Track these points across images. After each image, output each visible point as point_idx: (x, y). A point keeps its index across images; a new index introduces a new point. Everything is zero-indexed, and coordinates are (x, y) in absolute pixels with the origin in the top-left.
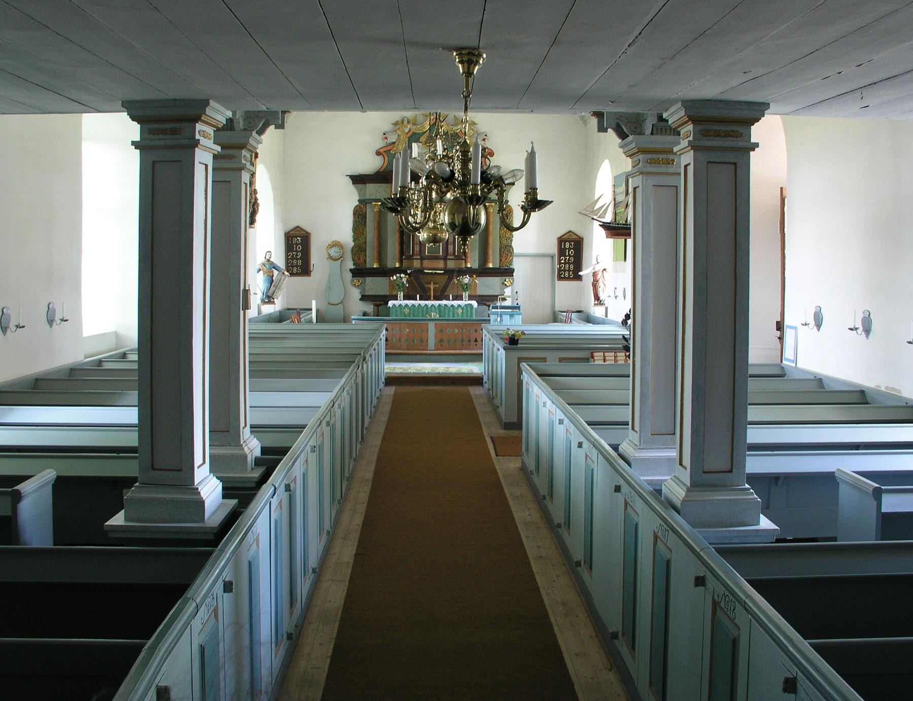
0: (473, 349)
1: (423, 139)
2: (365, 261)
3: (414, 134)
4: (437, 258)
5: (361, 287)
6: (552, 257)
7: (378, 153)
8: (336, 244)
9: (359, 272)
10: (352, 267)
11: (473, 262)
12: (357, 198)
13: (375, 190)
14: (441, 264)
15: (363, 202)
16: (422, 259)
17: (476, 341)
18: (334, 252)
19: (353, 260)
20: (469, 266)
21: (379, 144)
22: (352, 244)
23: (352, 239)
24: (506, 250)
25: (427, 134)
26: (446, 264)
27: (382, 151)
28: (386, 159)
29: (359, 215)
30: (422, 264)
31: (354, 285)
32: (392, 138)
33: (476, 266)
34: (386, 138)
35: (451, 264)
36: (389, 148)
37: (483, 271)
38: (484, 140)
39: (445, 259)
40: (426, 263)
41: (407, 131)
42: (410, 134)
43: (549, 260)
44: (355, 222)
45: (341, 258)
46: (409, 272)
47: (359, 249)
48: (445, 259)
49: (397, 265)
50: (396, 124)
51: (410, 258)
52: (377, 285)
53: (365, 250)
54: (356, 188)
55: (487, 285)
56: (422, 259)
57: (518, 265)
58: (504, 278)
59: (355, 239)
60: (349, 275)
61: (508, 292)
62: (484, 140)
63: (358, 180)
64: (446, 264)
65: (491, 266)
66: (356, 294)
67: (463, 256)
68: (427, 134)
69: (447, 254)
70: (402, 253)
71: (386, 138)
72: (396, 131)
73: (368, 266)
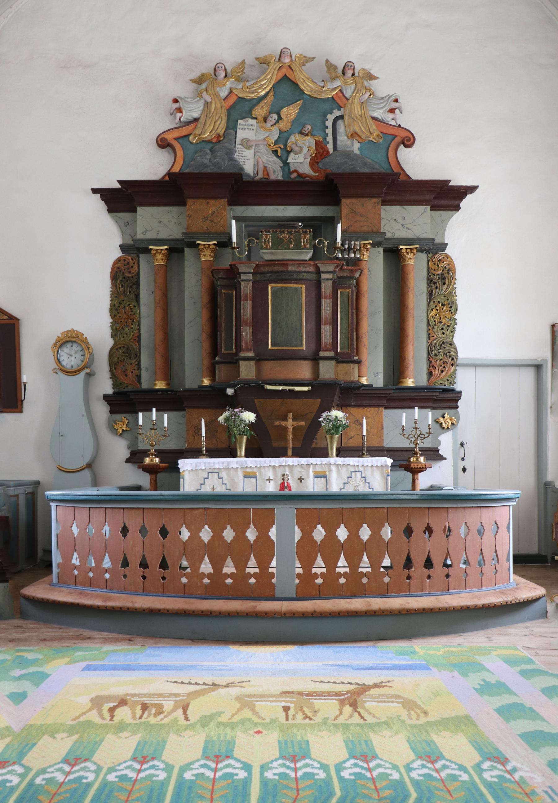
0: (421, 592)
1: (260, 111)
2: (139, 377)
3: (241, 99)
4: (295, 357)
5: (131, 433)
6: (538, 368)
7: (163, 143)
8: (70, 339)
9: (125, 401)
10: (109, 390)
11: (372, 372)
12: (118, 240)
13: (158, 222)
14: (304, 371)
15: (134, 249)
16: (262, 357)
17: (428, 564)
18: (70, 358)
19: (113, 376)
20: (364, 381)
21: (164, 124)
22: (110, 342)
23: (108, 331)
24: (442, 353)
25: (271, 97)
26: (316, 371)
27: (169, 137)
28: (180, 153)
29: (124, 280)
30: (258, 370)
31: (113, 430)
32: (193, 110)
33: (379, 382)
34: (179, 110)
35: (328, 371)
36: (184, 131)
37: (395, 395)
38: (392, 111)
39: (315, 359)
40: (272, 369)
41: (223, 93)
42: (233, 99)
43: (529, 375)
44: (115, 295)
45: (86, 369)
46: (230, 391)
47: (124, 354)
48: (315, 359)
49: (206, 382)
50: (200, 80)
51: (233, 361)
52: (156, 424)
53: (138, 356)
54: (112, 217)
55: (403, 423)
56: (262, 357)
57: (464, 381)
58: (441, 412)
59: (117, 330)
60: (102, 411)
61: (446, 443)
62: (392, 111)
63: (122, 199)
64: (316, 371)
65: (410, 383)
66: (119, 449)
67: (350, 356)
68: (271, 97)
69: (319, 346)
70: (214, 351)
71: (179, 110)
72: (200, 95)
73: (145, 385)
